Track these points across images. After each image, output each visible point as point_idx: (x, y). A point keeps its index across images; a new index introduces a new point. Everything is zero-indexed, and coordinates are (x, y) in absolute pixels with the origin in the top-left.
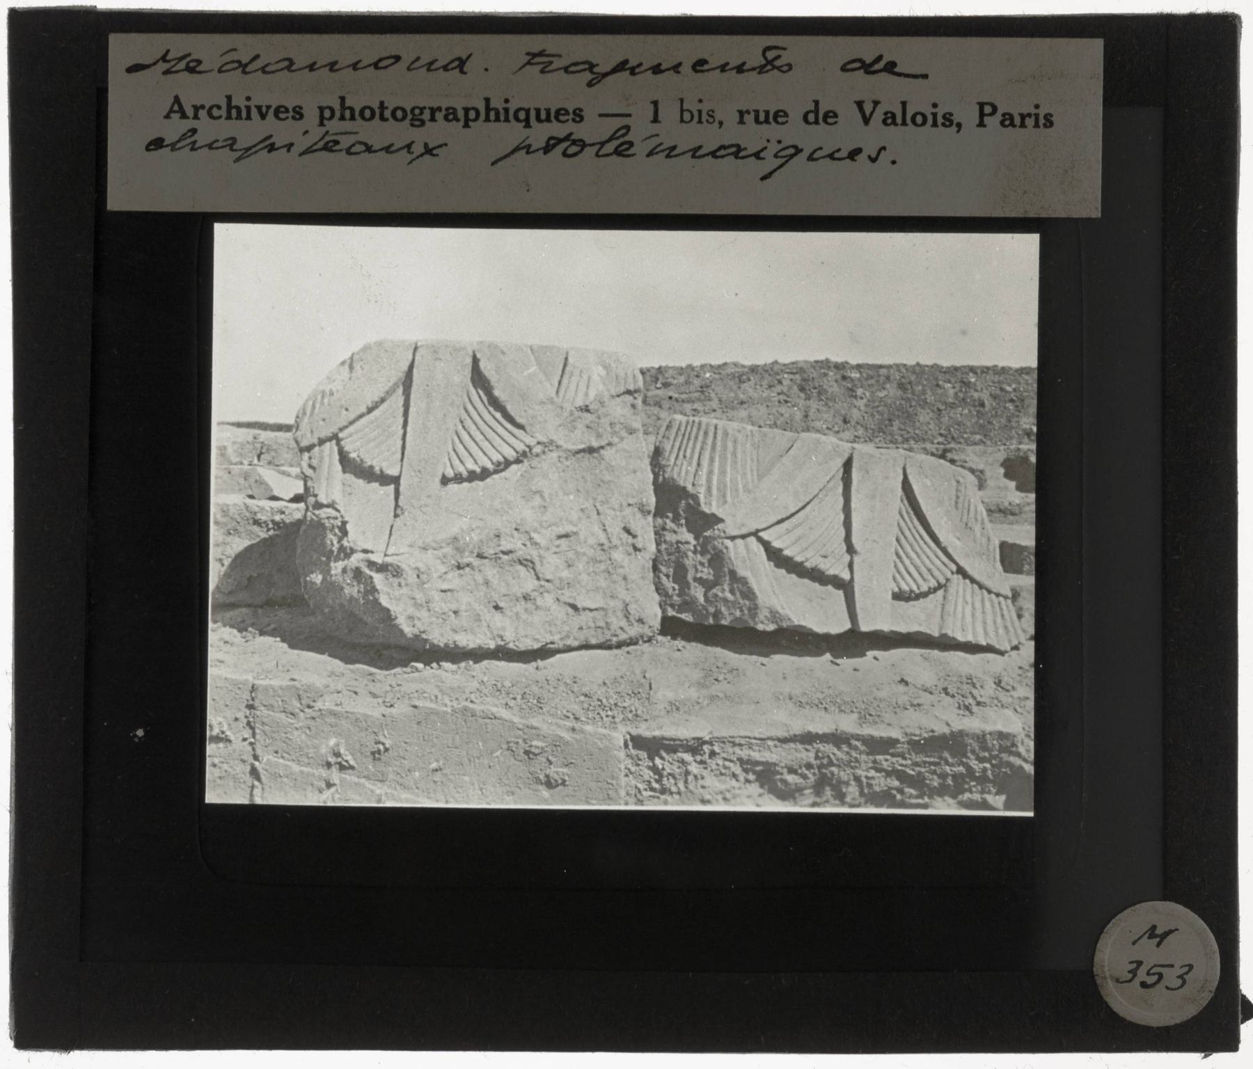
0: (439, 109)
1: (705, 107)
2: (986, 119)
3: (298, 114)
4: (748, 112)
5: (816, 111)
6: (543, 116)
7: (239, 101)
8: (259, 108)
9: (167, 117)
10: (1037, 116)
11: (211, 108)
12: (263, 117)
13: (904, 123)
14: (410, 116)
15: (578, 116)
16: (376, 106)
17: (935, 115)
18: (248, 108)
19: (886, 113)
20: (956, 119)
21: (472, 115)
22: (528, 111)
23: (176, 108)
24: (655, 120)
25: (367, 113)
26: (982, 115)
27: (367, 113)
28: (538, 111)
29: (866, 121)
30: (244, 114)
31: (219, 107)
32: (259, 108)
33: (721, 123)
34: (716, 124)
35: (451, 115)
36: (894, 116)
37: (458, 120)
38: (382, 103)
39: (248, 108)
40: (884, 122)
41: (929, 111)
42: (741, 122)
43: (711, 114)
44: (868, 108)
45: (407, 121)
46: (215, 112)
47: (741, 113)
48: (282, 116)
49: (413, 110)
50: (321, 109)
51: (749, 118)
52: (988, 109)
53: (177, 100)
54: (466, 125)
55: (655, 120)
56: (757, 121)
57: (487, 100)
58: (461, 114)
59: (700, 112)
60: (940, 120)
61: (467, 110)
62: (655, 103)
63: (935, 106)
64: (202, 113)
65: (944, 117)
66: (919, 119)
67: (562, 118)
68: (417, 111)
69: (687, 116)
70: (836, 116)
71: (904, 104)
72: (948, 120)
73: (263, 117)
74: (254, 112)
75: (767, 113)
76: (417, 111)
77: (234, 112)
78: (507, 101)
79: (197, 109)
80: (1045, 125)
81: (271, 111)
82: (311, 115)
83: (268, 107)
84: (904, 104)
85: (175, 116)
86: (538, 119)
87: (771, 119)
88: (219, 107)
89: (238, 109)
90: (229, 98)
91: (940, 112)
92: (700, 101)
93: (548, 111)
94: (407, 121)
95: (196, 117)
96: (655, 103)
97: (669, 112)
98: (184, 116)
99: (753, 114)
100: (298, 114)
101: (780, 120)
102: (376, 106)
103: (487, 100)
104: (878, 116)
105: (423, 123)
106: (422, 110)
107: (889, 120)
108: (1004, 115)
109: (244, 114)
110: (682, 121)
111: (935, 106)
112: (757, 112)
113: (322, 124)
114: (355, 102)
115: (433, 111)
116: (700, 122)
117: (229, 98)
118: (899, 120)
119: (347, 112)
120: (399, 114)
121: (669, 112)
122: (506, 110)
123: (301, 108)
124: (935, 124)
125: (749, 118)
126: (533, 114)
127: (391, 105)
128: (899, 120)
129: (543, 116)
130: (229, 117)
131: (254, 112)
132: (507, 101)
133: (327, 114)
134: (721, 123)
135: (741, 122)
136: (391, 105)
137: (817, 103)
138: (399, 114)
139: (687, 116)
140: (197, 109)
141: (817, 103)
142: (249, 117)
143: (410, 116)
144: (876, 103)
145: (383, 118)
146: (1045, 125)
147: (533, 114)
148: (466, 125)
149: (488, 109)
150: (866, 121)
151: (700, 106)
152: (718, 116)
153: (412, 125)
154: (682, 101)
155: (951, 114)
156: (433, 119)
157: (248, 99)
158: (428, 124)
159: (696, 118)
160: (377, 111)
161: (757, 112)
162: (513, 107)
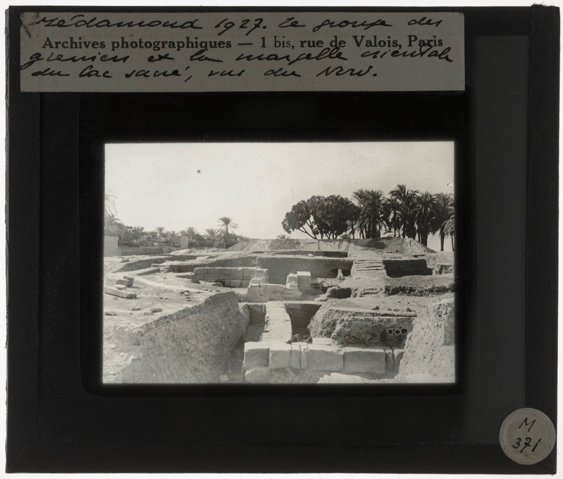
0: (166, 42)
1: (286, 40)
2: (413, 43)
3: (103, 45)
4: (305, 42)
5: (336, 41)
6: (213, 45)
7: (76, 40)
8: (85, 43)
9: (44, 47)
10: (435, 41)
11: (64, 43)
12: (87, 47)
13: (375, 45)
14: (153, 46)
15: (229, 45)
16: (138, 41)
17: (389, 42)
18: (80, 43)
19: (367, 41)
20: (398, 43)
21: (181, 45)
22: (206, 43)
23: (48, 43)
24: (264, 46)
25: (134, 45)
26: (410, 41)
27: (134, 45)
28: (211, 42)
29: (358, 44)
30: (78, 46)
31: (67, 43)
32: (85, 43)
33: (293, 47)
34: (291, 48)
35: (172, 45)
36: (371, 42)
37: (175, 47)
38: (140, 40)
39: (80, 43)
40: (367, 45)
41: (386, 40)
42: (302, 46)
43: (288, 43)
44: (359, 39)
45: (152, 48)
46: (66, 45)
47: (302, 43)
48: (95, 46)
49: (154, 43)
50: (113, 43)
51: (306, 45)
52: (413, 38)
53: (48, 38)
54: (179, 50)
55: (264, 46)
56: (309, 46)
57: (188, 38)
58: (176, 45)
59: (283, 42)
60: (392, 44)
61: (178, 43)
62: (263, 38)
63: (389, 37)
64: (60, 46)
65: (393, 42)
66: (382, 44)
67: (221, 46)
68: (156, 44)
69: (278, 44)
70: (345, 43)
71: (375, 37)
72: (395, 43)
73: (87, 47)
74: (83, 45)
75: (314, 42)
76: (156, 44)
77: (74, 45)
78: (196, 38)
79: (57, 43)
80: (439, 45)
81: (91, 44)
82: (109, 46)
83: (89, 42)
84: (375, 37)
85: (48, 47)
86: (211, 47)
87: (316, 45)
88: (67, 43)
89: (76, 43)
90: (72, 38)
91: (392, 40)
92: (284, 37)
93: (215, 42)
94: (152, 48)
95: (57, 47)
96: (263, 38)
97: (270, 42)
98: (51, 47)
99: (307, 43)
100: (103, 45)
101: (320, 45)
102: (138, 41)
103: (188, 38)
104: (364, 43)
105: (159, 49)
106: (158, 43)
107: (369, 44)
108: (420, 41)
109: (78, 46)
110: (275, 46)
111: (389, 37)
112: (309, 42)
113: (113, 50)
114: (128, 40)
115: (164, 43)
116: (284, 46)
117: (72, 38)
118: (373, 44)
119: (124, 44)
120: (148, 45)
121: (270, 42)
122: (196, 43)
123: (104, 42)
124: (389, 46)
125: (306, 45)
126: (208, 44)
127: (144, 41)
128: (373, 44)
129: (213, 45)
130: (72, 47)
131: (83, 45)
132: (196, 38)
133: (116, 45)
134: (293, 47)
135: (302, 46)
136: (144, 41)
137: (336, 37)
138: (148, 45)
139: (278, 44)
140: (57, 43)
141: (336, 37)
142: (80, 47)
143: (153, 46)
144: (363, 37)
145: (141, 47)
146: (439, 45)
147: (208, 44)
148: (179, 50)
149: (188, 42)
150: (358, 44)
151: (283, 39)
152: (292, 44)
153: (154, 50)
154: (275, 37)
155: (397, 41)
156: (163, 47)
157: (80, 39)
158: (161, 49)
159: (282, 45)
160: (138, 44)
161: (309, 42)
162: (199, 41)
